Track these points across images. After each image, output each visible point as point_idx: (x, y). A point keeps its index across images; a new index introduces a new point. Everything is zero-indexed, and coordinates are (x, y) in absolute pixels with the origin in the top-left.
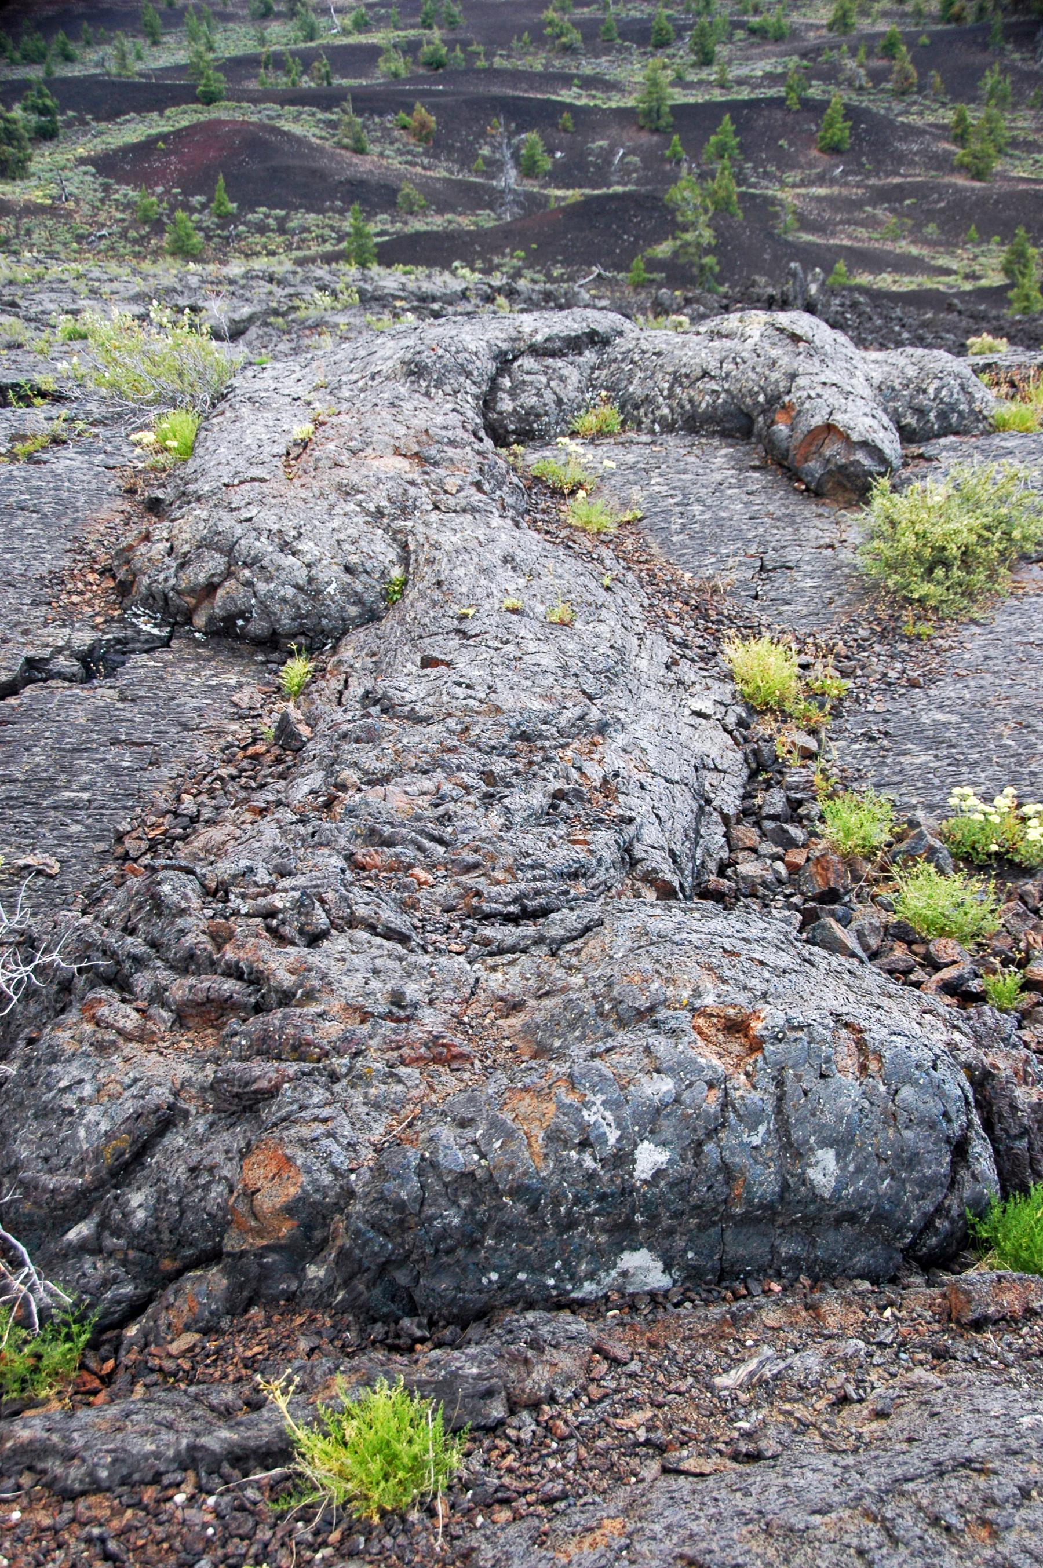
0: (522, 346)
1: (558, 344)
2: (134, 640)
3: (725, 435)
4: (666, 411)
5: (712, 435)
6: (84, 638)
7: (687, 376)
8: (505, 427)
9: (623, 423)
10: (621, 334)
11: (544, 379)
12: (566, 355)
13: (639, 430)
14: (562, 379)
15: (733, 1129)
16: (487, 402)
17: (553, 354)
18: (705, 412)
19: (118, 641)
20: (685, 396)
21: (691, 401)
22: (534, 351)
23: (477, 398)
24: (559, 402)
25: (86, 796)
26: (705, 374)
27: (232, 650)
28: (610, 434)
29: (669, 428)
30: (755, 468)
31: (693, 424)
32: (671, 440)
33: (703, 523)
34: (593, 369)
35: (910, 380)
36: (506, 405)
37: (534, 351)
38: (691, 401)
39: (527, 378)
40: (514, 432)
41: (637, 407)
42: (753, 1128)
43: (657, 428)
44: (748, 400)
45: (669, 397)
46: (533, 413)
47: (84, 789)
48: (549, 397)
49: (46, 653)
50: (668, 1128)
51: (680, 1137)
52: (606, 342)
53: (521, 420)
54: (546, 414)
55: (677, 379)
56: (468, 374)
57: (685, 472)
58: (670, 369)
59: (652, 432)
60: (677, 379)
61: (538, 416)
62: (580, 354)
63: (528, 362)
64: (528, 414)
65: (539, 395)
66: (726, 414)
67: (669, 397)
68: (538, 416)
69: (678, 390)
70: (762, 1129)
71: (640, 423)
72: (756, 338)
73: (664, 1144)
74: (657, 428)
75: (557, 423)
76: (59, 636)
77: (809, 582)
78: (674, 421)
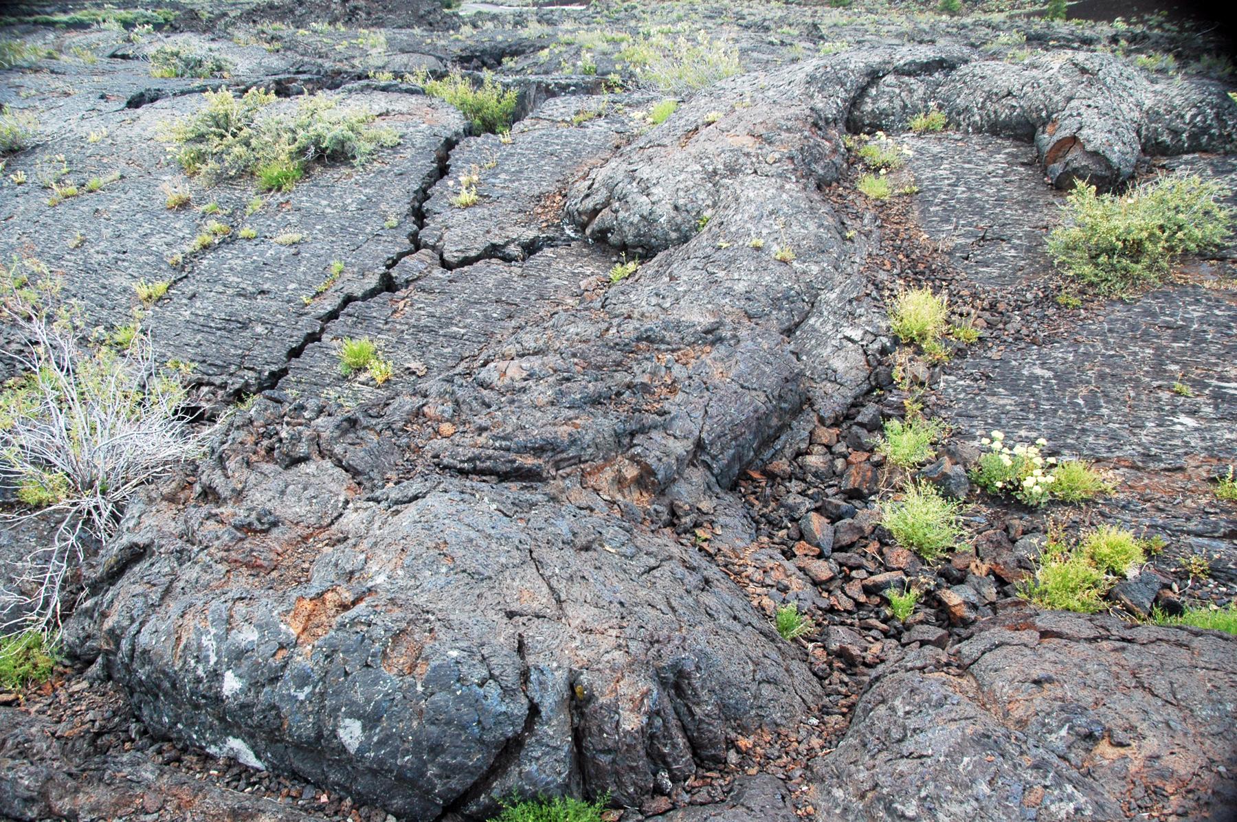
0: (891, 68)
1: (913, 67)
2: (558, 239)
3: (1016, 138)
4: (977, 118)
5: (1008, 137)
6: (530, 234)
7: (996, 94)
8: (862, 121)
9: (946, 126)
10: (966, 62)
11: (897, 91)
12: (919, 75)
13: (958, 130)
14: (911, 91)
15: (286, 683)
16: (855, 102)
17: (909, 74)
18: (1004, 121)
19: (549, 238)
20: (992, 109)
21: (995, 112)
22: (899, 72)
23: (845, 100)
24: (905, 106)
25: (462, 331)
26: (1009, 93)
27: (604, 252)
28: (934, 131)
29: (978, 130)
30: (1023, 164)
31: (995, 128)
32: (975, 139)
33: (959, 201)
34: (938, 85)
35: (1174, 108)
36: (868, 107)
37: (899, 72)
38: (995, 112)
39: (887, 89)
40: (868, 125)
41: (959, 114)
42: (300, 687)
43: (970, 129)
44: (1034, 115)
45: (981, 108)
46: (884, 113)
47: (465, 327)
48: (897, 103)
49: (501, 242)
50: (245, 665)
51: (250, 676)
52: (953, 67)
53: (875, 117)
54: (893, 114)
55: (989, 95)
56: (843, 85)
57: (969, 162)
58: (987, 89)
59: (967, 132)
60: (989, 95)
61: (887, 115)
62: (931, 75)
63: (890, 79)
64: (881, 114)
65: (891, 101)
66: (1018, 123)
67: (981, 108)
68: (887, 115)
69: (988, 104)
70: (307, 690)
71: (959, 125)
72: (1055, 70)
73: (240, 676)
74: (970, 129)
75: (900, 121)
76: (514, 232)
77: (1013, 252)
78: (982, 126)
